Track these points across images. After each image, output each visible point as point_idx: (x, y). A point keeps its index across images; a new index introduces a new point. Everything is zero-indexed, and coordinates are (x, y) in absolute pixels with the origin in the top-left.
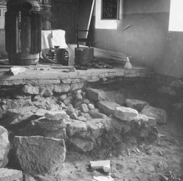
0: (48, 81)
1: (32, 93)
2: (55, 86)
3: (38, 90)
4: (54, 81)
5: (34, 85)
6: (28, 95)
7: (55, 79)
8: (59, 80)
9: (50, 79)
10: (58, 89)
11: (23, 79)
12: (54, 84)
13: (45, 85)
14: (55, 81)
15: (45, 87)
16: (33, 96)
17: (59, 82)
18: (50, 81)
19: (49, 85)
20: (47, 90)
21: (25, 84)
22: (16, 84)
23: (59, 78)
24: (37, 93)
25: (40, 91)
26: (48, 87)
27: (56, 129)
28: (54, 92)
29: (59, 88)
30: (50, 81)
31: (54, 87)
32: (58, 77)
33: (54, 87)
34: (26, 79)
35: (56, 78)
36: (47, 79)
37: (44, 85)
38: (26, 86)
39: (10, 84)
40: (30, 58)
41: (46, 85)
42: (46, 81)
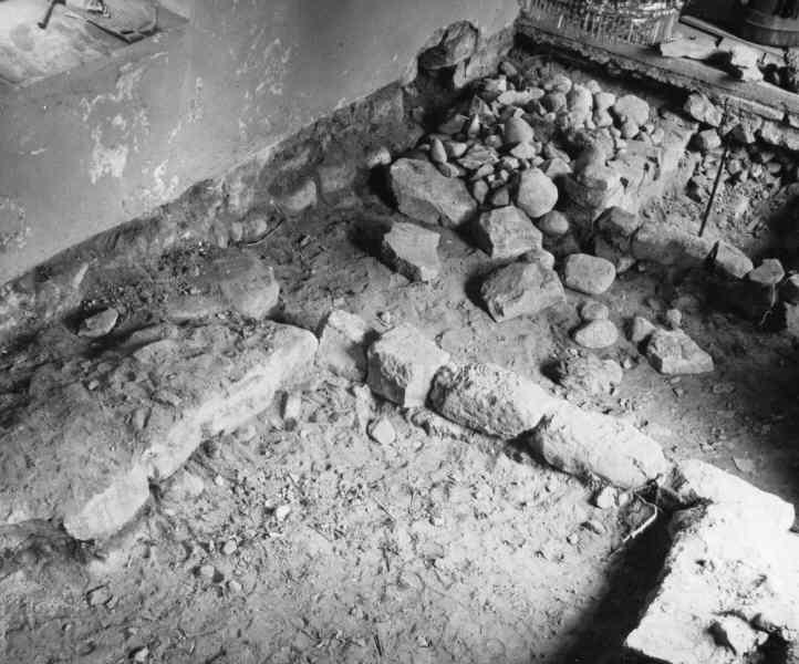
0: (753, 103)
1: (700, 118)
2: (766, 123)
3: (720, 117)
4: (766, 108)
5: (714, 101)
6: (689, 118)
7: (772, 107)
8: (782, 111)
9: (758, 101)
10: (772, 134)
11: (695, 79)
12: (765, 119)
13: (741, 110)
14: (771, 110)
15: (740, 116)
16: (705, 126)
17: (781, 116)
18: (757, 107)
19: (749, 115)
20: (740, 126)
21: (695, 91)
22: (673, 82)
23: (782, 107)
24: (716, 123)
25: (725, 119)
26: (746, 120)
27: (583, 204)
28: (757, 134)
29: (775, 134)
30: (757, 107)
31: (763, 125)
32: (782, 103)
33: (763, 125)
34: (702, 82)
35: (774, 103)
36: (751, 100)
37: (737, 111)
38: (692, 98)
39: (662, 79)
40: (771, 27)
41: (743, 114)
42: (746, 101)
